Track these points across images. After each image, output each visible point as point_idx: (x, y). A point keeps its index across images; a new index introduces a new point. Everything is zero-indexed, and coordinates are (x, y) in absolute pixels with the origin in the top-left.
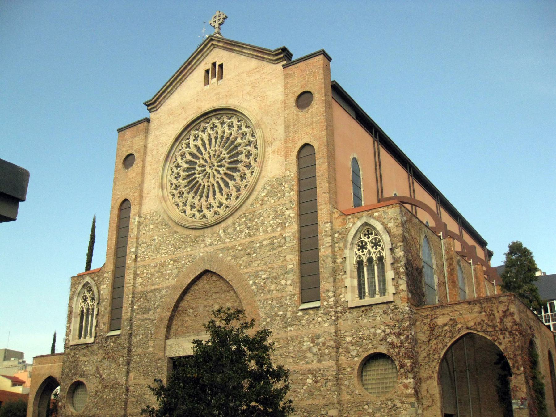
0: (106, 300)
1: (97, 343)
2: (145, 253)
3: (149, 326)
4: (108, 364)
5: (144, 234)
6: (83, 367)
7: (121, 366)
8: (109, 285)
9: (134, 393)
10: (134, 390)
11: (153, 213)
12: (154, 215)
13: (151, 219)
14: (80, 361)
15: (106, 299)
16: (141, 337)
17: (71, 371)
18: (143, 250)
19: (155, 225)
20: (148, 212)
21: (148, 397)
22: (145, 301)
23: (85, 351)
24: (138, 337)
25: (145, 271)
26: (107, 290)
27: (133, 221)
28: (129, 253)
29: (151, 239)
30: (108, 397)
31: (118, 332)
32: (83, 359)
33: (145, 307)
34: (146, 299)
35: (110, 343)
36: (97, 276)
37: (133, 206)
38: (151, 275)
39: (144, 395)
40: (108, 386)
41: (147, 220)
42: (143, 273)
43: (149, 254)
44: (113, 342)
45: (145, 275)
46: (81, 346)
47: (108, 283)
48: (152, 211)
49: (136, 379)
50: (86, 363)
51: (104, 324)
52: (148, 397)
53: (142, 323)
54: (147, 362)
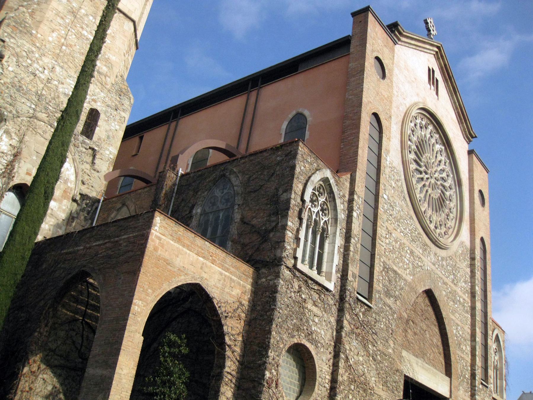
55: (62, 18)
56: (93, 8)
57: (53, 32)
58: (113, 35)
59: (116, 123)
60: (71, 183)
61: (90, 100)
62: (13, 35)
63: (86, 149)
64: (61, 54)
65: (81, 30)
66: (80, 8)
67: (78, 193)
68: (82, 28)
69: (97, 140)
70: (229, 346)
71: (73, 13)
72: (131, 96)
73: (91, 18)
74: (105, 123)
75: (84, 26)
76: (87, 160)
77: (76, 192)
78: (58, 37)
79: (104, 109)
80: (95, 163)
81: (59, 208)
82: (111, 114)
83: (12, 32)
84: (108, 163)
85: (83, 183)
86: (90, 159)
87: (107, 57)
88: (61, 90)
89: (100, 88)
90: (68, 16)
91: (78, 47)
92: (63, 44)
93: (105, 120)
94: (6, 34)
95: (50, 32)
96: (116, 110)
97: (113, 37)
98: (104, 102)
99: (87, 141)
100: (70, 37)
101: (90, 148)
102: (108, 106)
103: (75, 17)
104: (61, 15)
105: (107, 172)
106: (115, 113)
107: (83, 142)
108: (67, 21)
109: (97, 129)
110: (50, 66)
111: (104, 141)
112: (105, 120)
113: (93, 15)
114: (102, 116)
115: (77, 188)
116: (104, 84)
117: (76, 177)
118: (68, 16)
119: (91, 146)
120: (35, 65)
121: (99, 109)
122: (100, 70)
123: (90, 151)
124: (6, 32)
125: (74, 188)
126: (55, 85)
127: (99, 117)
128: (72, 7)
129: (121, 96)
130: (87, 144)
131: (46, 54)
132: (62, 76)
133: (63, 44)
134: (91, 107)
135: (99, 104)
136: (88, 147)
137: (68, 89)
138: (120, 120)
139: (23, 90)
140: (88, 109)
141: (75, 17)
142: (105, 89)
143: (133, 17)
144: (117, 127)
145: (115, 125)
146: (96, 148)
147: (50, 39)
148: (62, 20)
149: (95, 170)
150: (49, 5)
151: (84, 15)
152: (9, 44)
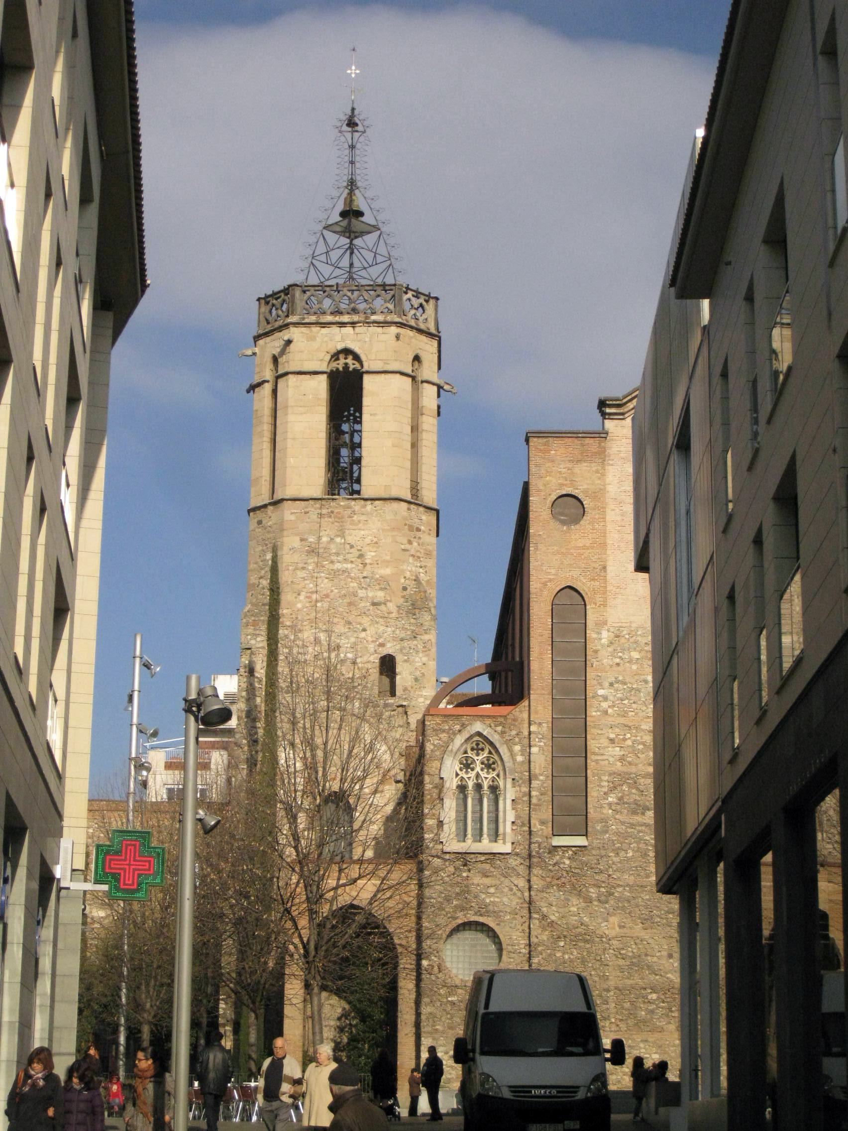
0: (541, 778)
1: (517, 854)
2: (626, 702)
3: (647, 838)
4: (563, 897)
5: (618, 664)
6: (483, 896)
7: (596, 903)
8: (545, 748)
9: (623, 952)
10: (621, 946)
11: (637, 629)
12: (639, 633)
13: (632, 640)
14: (473, 884)
15: (541, 775)
16: (630, 854)
17: (448, 900)
18: (619, 695)
19: (643, 654)
20: (624, 625)
21: (655, 959)
22: (634, 791)
23: (487, 866)
24: (622, 854)
25: (628, 736)
26: (543, 758)
27: (594, 636)
28: (593, 697)
29: (636, 677)
30: (566, 957)
31: (580, 841)
32: (481, 882)
33: (636, 802)
34: (638, 789)
35: (562, 858)
36: (501, 724)
37: (594, 606)
38: (644, 745)
39: (646, 955)
40: (565, 937)
41: (623, 640)
42: (625, 740)
43: (634, 706)
44: (569, 858)
45: (629, 743)
46: (472, 856)
47: (542, 744)
48: (634, 625)
49: (624, 927)
50: (492, 890)
51: (543, 823)
52: (655, 959)
53: (629, 830)
54: (649, 900)
55: (303, 568)
56: (337, 524)
57: (299, 594)
58: (375, 540)
59: (421, 655)
62: (257, 632)
65: (331, 567)
68: (332, 562)
69: (402, 692)
70: (400, 945)
71: (313, 551)
73: (338, 540)
74: (405, 665)
75: (334, 558)
78: (307, 597)
83: (255, 630)
87: (378, 576)
89: (383, 623)
90: (309, 561)
91: (336, 591)
92: (317, 601)
93: (406, 661)
94: (249, 637)
95: (296, 598)
96: (415, 637)
97: (376, 543)
98: (394, 639)
100: (322, 586)
101: (398, 707)
102: (402, 640)
103: (318, 554)
104: (300, 565)
106: (415, 642)
107: (386, 705)
108: (310, 568)
110: (312, 639)
111: (412, 687)
112: (406, 661)
113: (339, 533)
116: (386, 615)
118: (309, 561)
119: (397, 704)
120: (295, 650)
121: (391, 652)
123: (400, 709)
124: (248, 635)
128: (309, 544)
129: (414, 614)
130: (392, 705)
133: (317, 601)
134: (380, 656)
135: (389, 645)
140: (377, 661)
141: (318, 554)
142: (390, 620)
143: (394, 493)
144: (425, 659)
145: (421, 658)
146: (404, 703)
147: (299, 606)
148: (304, 571)
151: (328, 543)
152: (258, 646)
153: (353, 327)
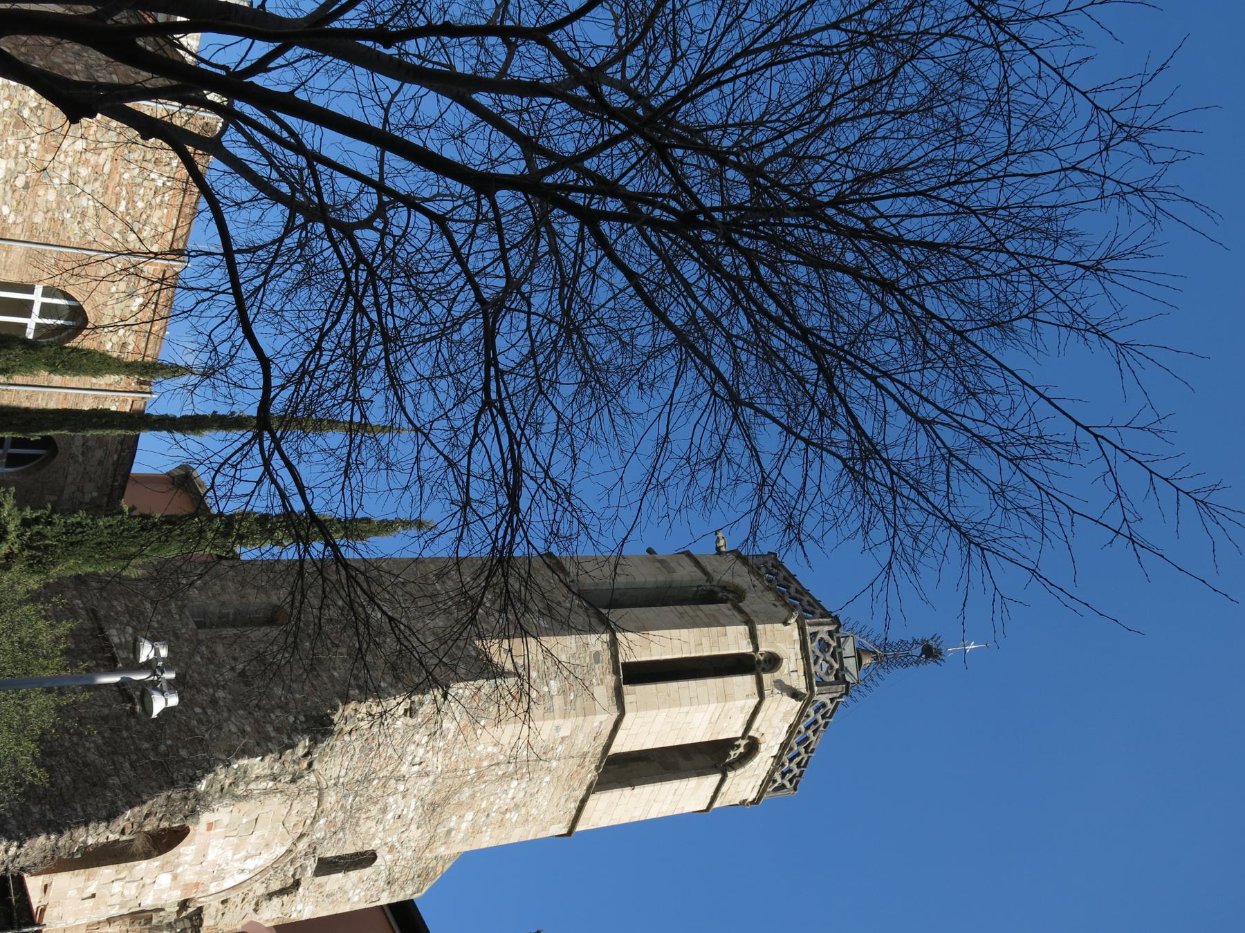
58: (530, 819)
59: (363, 894)
60: (218, 885)
61: (389, 845)
63: (293, 876)
64: (459, 773)
66: (559, 759)
67: (199, 905)
72: (426, 889)
76: (272, 885)
77: (202, 899)
79: (383, 868)
80: (270, 900)
81: (162, 891)
82: (376, 881)
84: (280, 915)
85: (224, 902)
86: (276, 886)
88: (391, 799)
96: (389, 883)
98: (395, 862)
99: (310, 872)
105: (261, 922)
109: (340, 875)
114: (367, 871)
115: (211, 897)
117: (233, 888)
122: (454, 832)
125: (209, 893)
126: (396, 789)
127: (364, 867)
130: (302, 874)
131: (449, 755)
132: (419, 790)
135: (389, 857)
136: (297, 877)
137: (398, 807)
138: (372, 896)
139: (368, 755)
149: (257, 904)
150: (544, 719)
153: (775, 757)
